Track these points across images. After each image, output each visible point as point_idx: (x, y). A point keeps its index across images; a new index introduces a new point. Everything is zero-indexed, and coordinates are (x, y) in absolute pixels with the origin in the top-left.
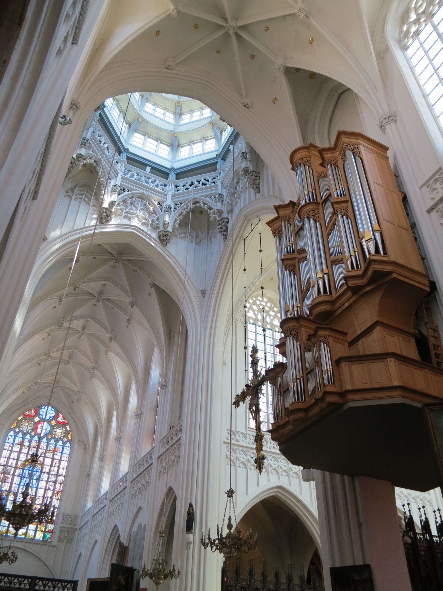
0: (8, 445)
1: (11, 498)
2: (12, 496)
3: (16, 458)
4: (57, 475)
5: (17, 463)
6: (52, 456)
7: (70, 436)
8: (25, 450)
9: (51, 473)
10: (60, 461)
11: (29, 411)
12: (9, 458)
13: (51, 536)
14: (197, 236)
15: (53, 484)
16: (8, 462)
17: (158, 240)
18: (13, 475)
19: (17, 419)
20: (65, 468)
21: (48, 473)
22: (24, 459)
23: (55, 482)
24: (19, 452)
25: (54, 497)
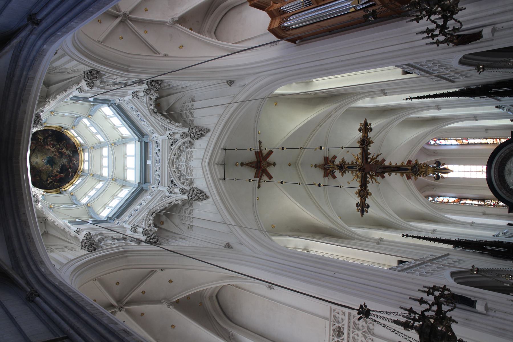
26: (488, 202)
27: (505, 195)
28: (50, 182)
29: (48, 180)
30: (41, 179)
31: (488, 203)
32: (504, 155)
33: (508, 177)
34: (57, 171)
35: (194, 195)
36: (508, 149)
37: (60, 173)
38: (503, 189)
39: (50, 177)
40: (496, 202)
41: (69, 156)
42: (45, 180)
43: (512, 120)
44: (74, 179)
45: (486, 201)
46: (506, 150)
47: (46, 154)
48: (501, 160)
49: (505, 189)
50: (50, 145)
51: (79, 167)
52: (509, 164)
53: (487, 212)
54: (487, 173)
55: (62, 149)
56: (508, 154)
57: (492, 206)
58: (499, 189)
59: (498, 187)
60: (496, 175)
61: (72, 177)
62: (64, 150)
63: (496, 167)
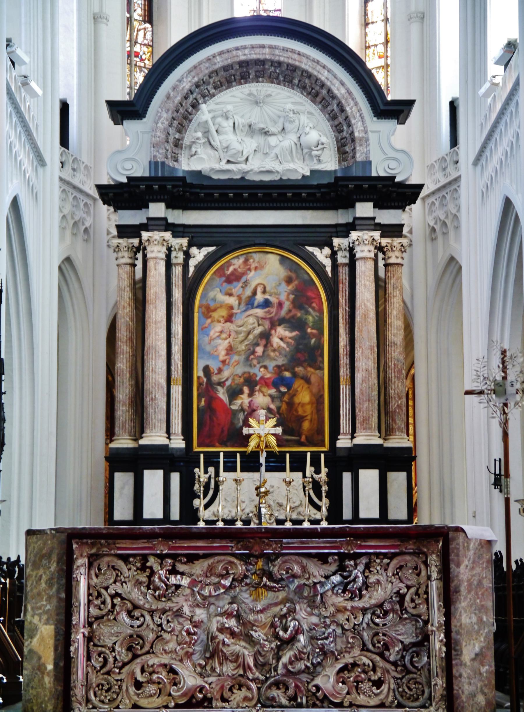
26: (145, 34)
27: (174, 88)
31: (141, 33)
32: (323, 78)
33: (241, 95)
36: (349, 93)
38: (196, 79)
40: (147, 62)
43: (455, 104)
45: (148, 25)
46: (343, 84)
48: (303, 71)
49: (197, 86)
52: (290, 97)
53: (103, 27)
54: (258, 18)
56: (329, 91)
57: (129, 49)
58: (195, 67)
59: (200, 63)
60: (247, 51)
63: (277, 52)
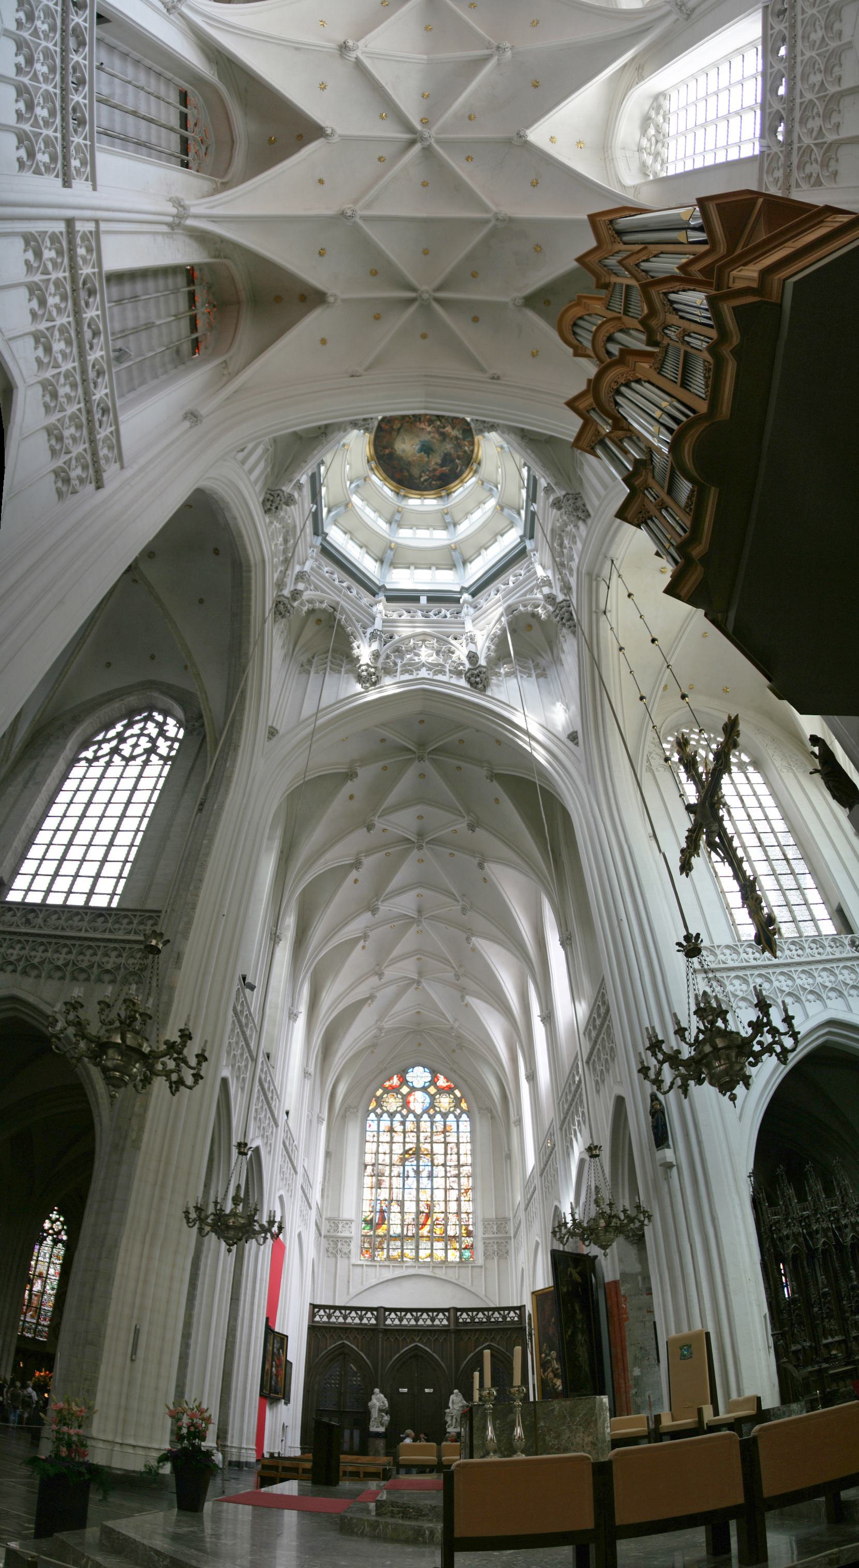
0: (372, 1134)
1: (395, 1208)
2: (396, 1206)
3: (388, 1151)
4: (459, 1166)
5: (391, 1158)
6: (443, 1140)
7: (464, 1105)
8: (398, 1138)
9: (448, 1163)
10: (458, 1144)
11: (389, 1080)
12: (377, 1153)
13: (472, 1253)
14: (537, 666)
15: (455, 1179)
16: (377, 1159)
17: (468, 686)
18: (391, 1177)
19: (375, 1096)
20: (469, 1152)
21: (444, 1165)
22: (401, 1151)
23: (458, 1176)
24: (391, 1142)
25: (462, 1198)
28: (426, 480)
29: (421, 477)
30: (411, 475)
34: (436, 464)
35: (558, 618)
37: (442, 466)
39: (423, 471)
41: (457, 438)
42: (417, 476)
44: (465, 475)
47: (418, 436)
50: (424, 422)
51: (474, 456)
55: (444, 427)
61: (462, 472)
62: (448, 429)
